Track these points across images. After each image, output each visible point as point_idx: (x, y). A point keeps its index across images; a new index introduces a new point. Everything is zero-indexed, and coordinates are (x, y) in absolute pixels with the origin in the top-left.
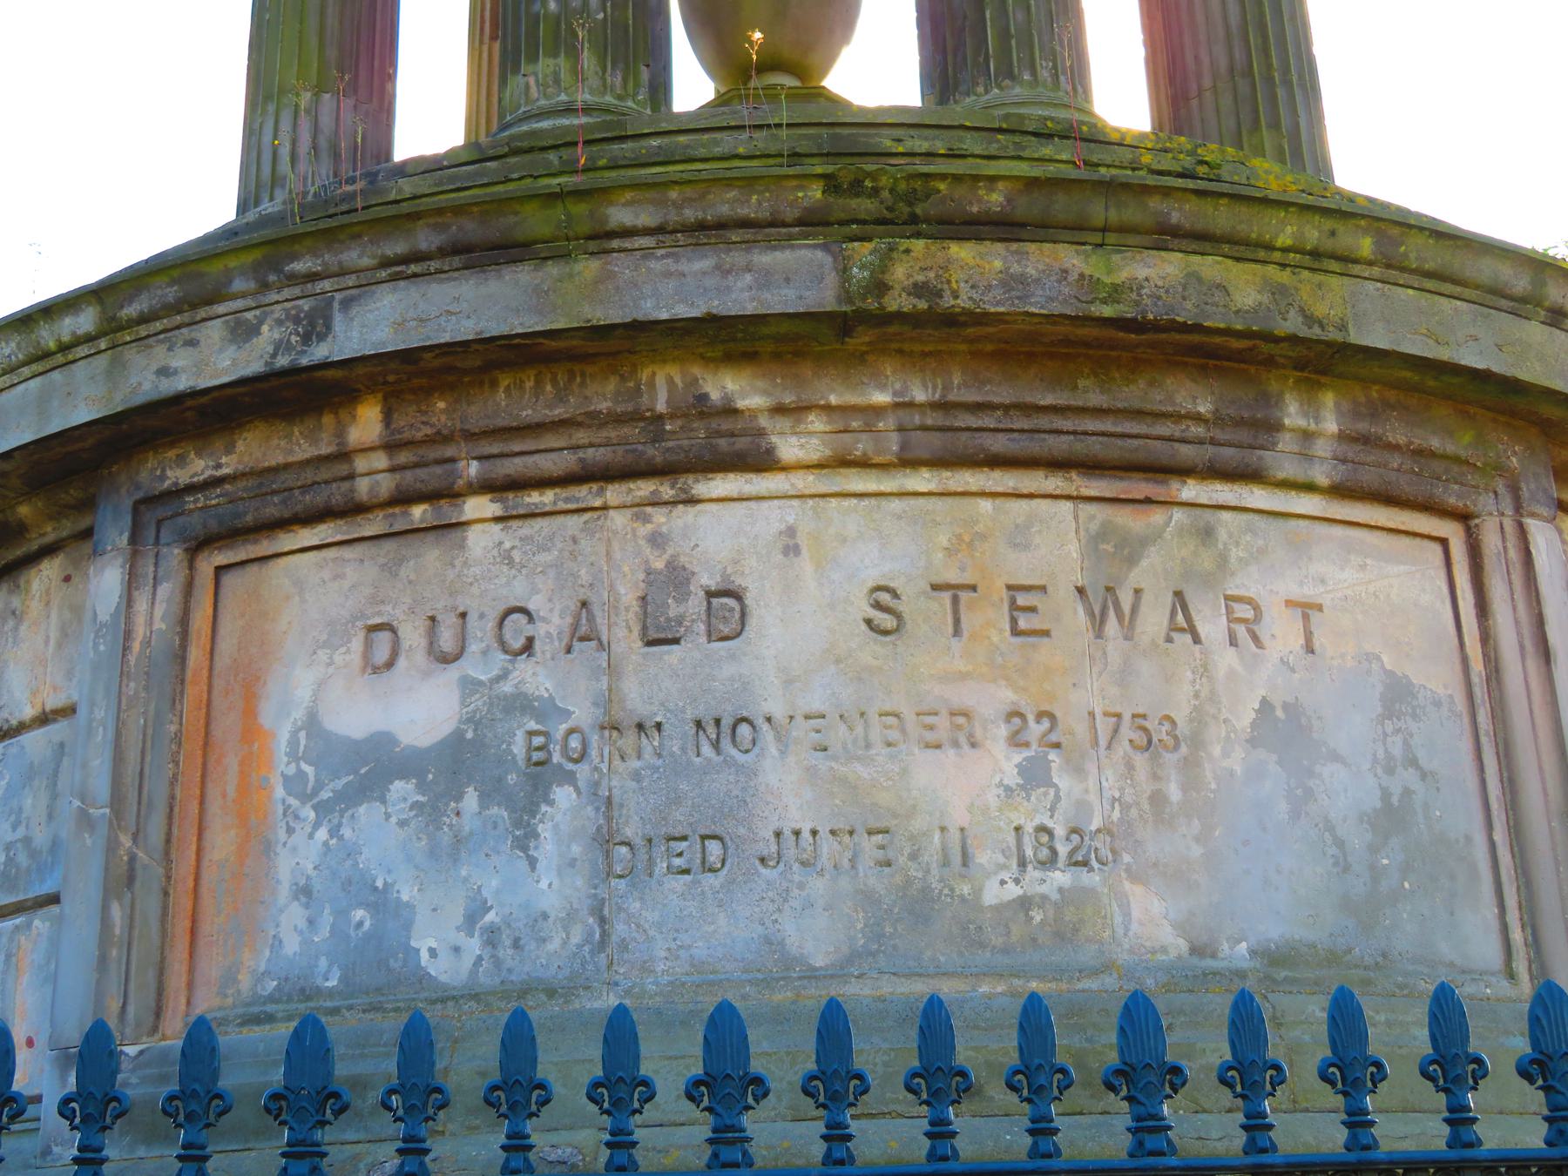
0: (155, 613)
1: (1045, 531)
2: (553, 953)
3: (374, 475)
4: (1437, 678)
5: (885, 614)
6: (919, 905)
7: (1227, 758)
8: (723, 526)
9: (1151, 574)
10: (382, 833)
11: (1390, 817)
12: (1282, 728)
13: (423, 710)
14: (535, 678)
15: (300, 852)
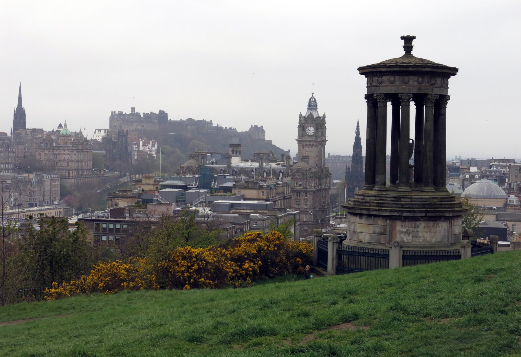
0: (391, 223)
1: (431, 223)
2: (410, 241)
3: (403, 219)
4: (447, 228)
5: (425, 227)
6: (425, 240)
7: (438, 233)
8: (418, 223)
9: (435, 225)
10: (402, 235)
11: (444, 235)
12: (440, 232)
13: (404, 230)
14: (410, 229)
15: (398, 235)
